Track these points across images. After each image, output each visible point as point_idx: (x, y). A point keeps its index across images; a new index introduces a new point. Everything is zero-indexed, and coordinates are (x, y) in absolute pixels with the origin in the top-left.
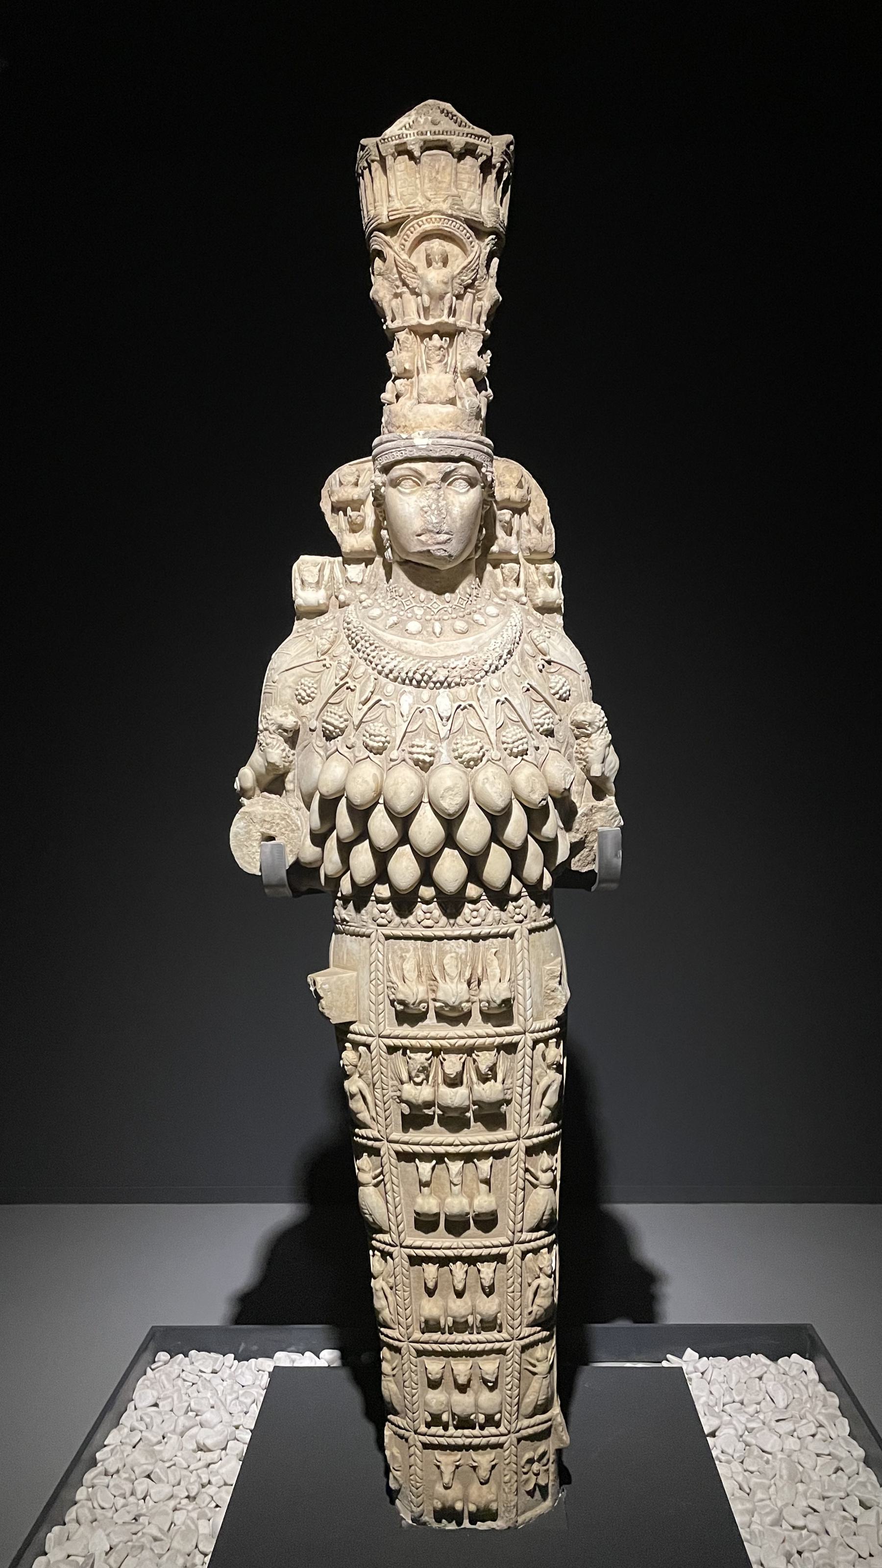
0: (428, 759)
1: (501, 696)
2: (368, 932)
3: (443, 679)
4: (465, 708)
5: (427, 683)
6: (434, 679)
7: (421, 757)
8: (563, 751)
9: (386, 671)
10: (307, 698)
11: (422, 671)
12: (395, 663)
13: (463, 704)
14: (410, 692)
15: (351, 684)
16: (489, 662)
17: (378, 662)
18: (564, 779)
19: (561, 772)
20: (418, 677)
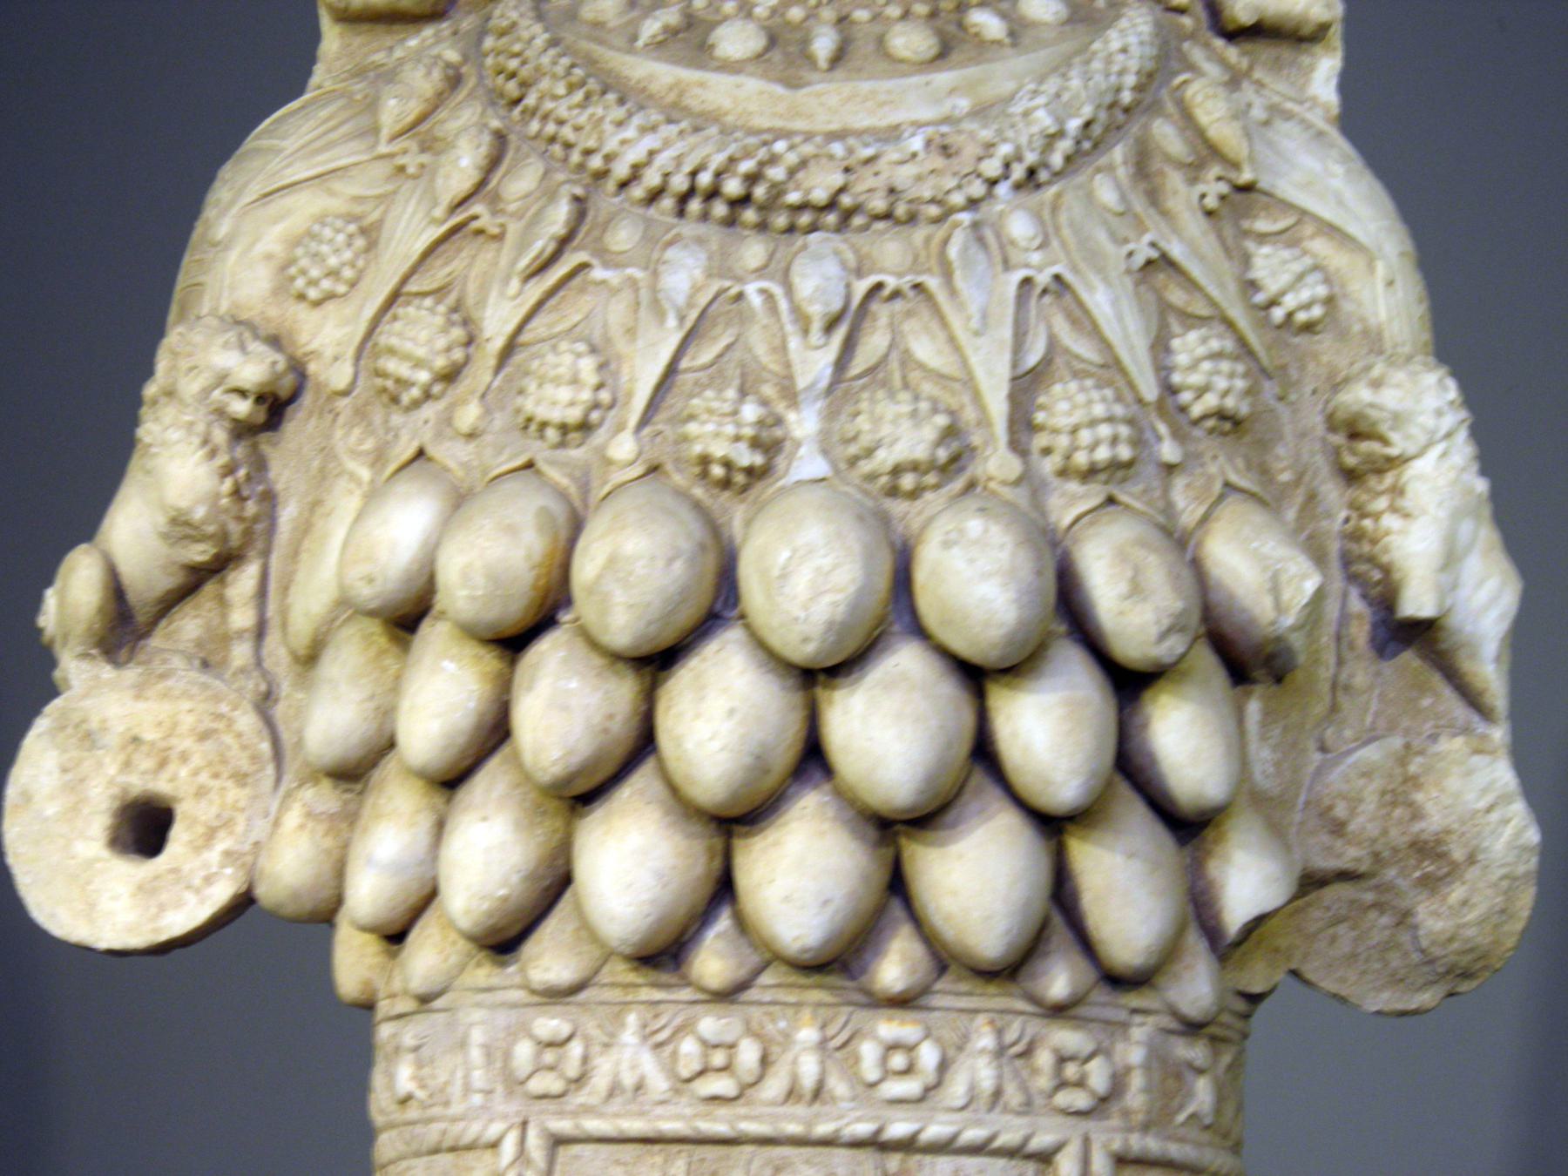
0: (746, 457)
1: (1040, 269)
2: (494, 1130)
3: (820, 196)
4: (896, 294)
5: (764, 208)
6: (793, 197)
7: (719, 450)
8: (1291, 514)
9: (621, 170)
10: (326, 284)
11: (746, 166)
12: (650, 142)
13: (891, 282)
14: (700, 241)
15: (486, 221)
16: (1005, 149)
17: (591, 144)
18: (1275, 589)
19: (1263, 571)
20: (733, 187)
